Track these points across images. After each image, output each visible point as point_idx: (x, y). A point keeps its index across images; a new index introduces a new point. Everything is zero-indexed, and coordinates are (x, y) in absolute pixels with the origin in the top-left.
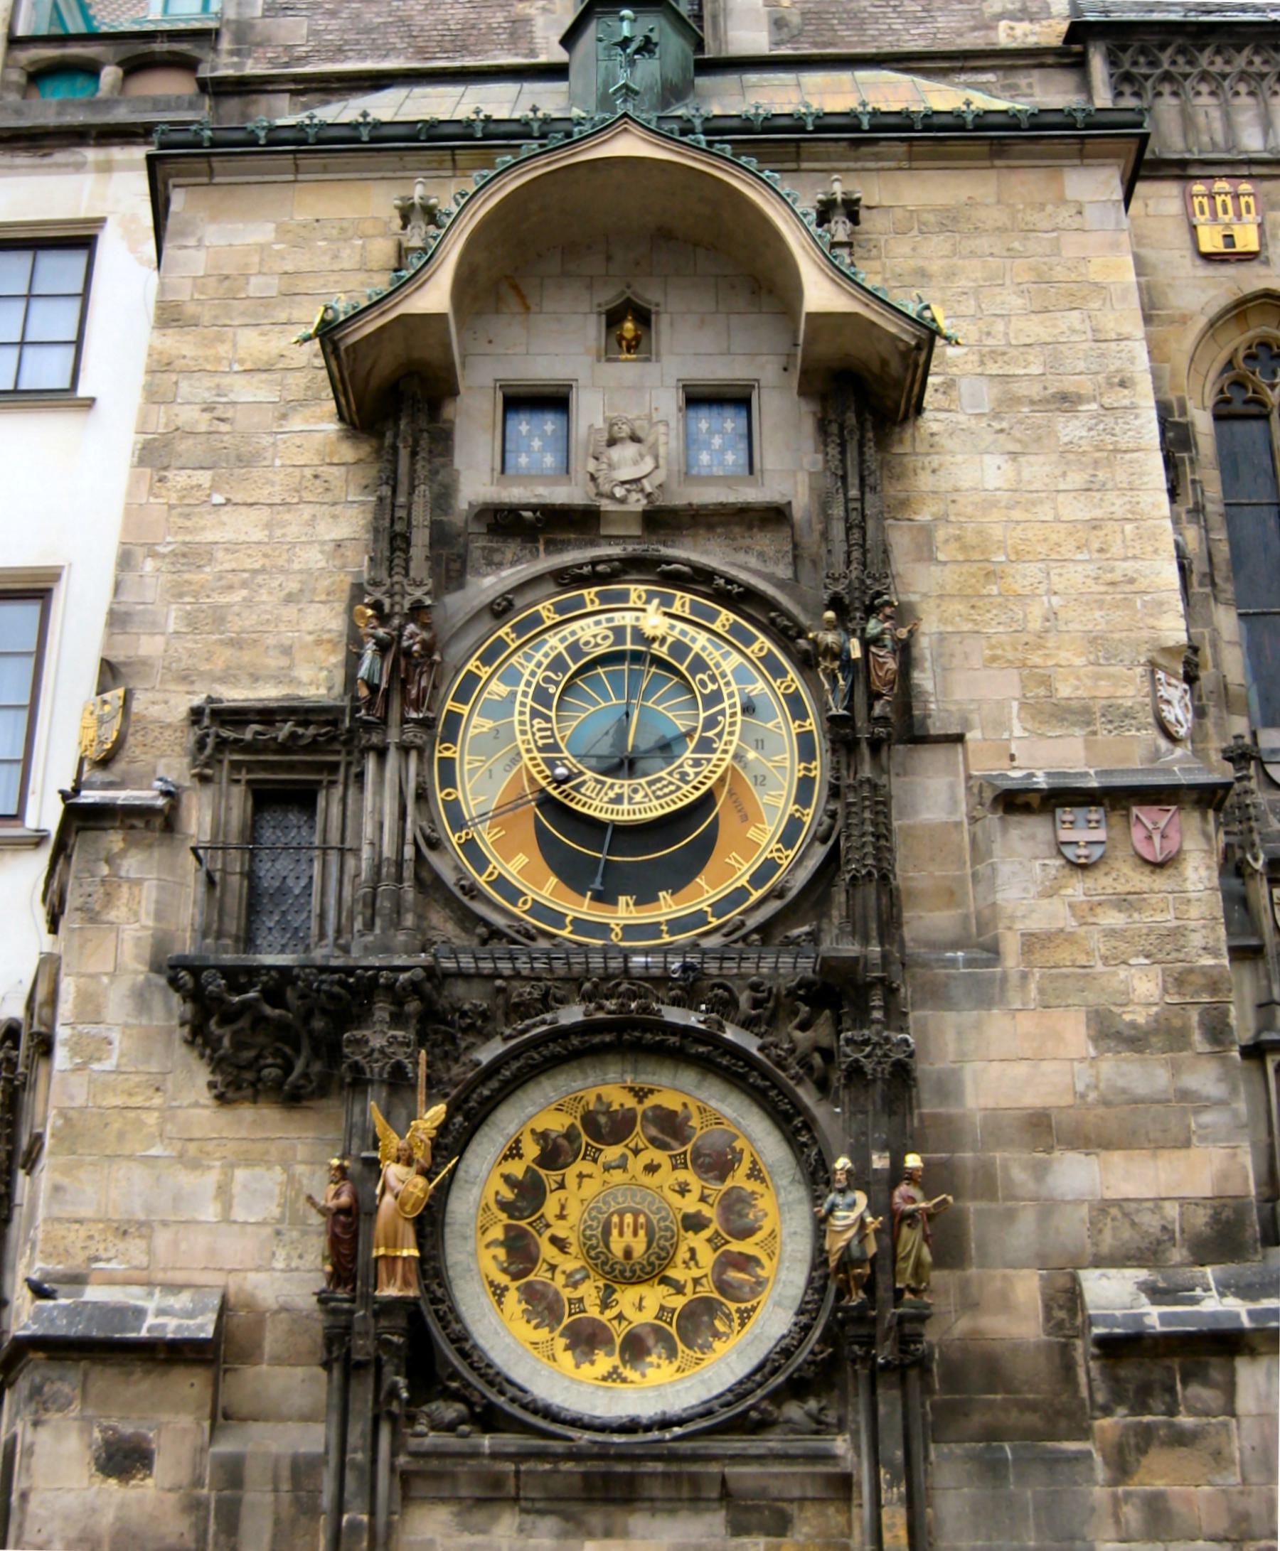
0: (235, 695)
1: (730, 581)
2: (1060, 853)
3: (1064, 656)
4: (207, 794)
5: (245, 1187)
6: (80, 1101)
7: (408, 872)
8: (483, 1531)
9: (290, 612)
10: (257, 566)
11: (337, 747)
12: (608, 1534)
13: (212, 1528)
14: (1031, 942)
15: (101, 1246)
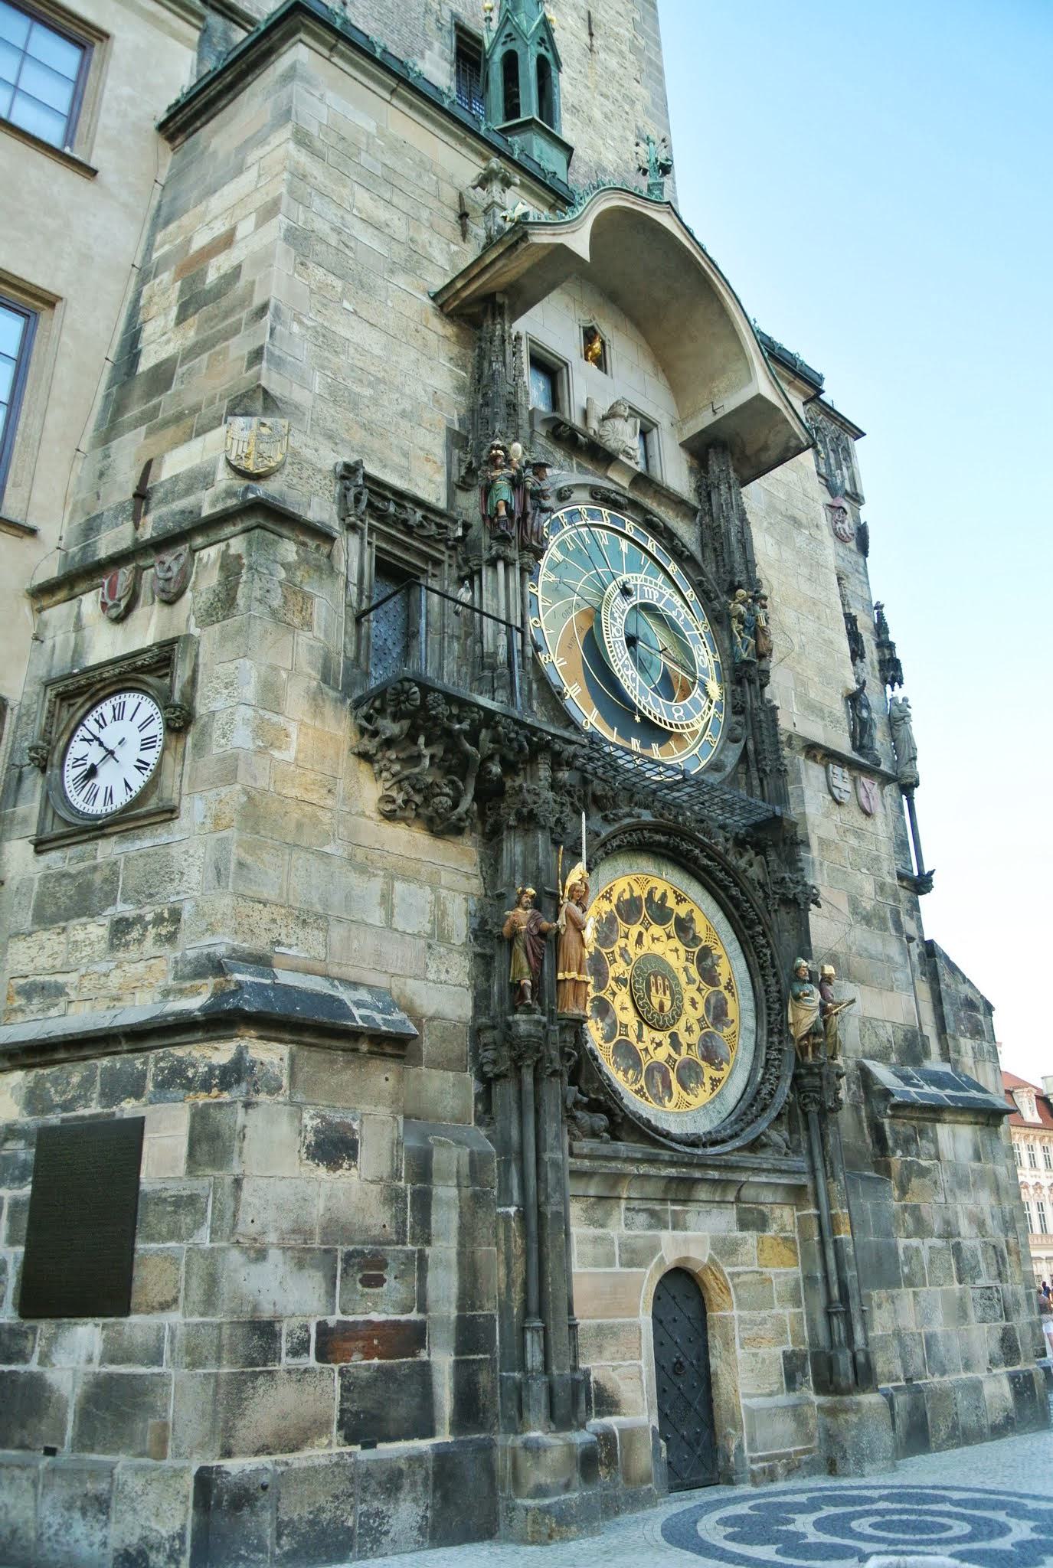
0: (371, 469)
1: (684, 546)
2: (831, 793)
3: (810, 673)
4: (354, 541)
5: (403, 900)
6: (262, 783)
7: (529, 668)
8: (602, 1226)
9: (404, 424)
10: (381, 375)
11: (443, 548)
12: (674, 1228)
13: (409, 1220)
14: (822, 841)
15: (284, 931)
